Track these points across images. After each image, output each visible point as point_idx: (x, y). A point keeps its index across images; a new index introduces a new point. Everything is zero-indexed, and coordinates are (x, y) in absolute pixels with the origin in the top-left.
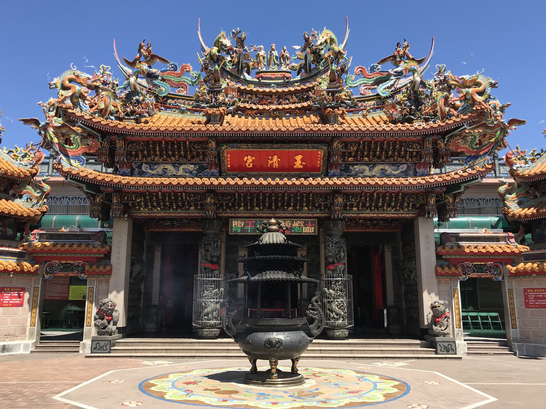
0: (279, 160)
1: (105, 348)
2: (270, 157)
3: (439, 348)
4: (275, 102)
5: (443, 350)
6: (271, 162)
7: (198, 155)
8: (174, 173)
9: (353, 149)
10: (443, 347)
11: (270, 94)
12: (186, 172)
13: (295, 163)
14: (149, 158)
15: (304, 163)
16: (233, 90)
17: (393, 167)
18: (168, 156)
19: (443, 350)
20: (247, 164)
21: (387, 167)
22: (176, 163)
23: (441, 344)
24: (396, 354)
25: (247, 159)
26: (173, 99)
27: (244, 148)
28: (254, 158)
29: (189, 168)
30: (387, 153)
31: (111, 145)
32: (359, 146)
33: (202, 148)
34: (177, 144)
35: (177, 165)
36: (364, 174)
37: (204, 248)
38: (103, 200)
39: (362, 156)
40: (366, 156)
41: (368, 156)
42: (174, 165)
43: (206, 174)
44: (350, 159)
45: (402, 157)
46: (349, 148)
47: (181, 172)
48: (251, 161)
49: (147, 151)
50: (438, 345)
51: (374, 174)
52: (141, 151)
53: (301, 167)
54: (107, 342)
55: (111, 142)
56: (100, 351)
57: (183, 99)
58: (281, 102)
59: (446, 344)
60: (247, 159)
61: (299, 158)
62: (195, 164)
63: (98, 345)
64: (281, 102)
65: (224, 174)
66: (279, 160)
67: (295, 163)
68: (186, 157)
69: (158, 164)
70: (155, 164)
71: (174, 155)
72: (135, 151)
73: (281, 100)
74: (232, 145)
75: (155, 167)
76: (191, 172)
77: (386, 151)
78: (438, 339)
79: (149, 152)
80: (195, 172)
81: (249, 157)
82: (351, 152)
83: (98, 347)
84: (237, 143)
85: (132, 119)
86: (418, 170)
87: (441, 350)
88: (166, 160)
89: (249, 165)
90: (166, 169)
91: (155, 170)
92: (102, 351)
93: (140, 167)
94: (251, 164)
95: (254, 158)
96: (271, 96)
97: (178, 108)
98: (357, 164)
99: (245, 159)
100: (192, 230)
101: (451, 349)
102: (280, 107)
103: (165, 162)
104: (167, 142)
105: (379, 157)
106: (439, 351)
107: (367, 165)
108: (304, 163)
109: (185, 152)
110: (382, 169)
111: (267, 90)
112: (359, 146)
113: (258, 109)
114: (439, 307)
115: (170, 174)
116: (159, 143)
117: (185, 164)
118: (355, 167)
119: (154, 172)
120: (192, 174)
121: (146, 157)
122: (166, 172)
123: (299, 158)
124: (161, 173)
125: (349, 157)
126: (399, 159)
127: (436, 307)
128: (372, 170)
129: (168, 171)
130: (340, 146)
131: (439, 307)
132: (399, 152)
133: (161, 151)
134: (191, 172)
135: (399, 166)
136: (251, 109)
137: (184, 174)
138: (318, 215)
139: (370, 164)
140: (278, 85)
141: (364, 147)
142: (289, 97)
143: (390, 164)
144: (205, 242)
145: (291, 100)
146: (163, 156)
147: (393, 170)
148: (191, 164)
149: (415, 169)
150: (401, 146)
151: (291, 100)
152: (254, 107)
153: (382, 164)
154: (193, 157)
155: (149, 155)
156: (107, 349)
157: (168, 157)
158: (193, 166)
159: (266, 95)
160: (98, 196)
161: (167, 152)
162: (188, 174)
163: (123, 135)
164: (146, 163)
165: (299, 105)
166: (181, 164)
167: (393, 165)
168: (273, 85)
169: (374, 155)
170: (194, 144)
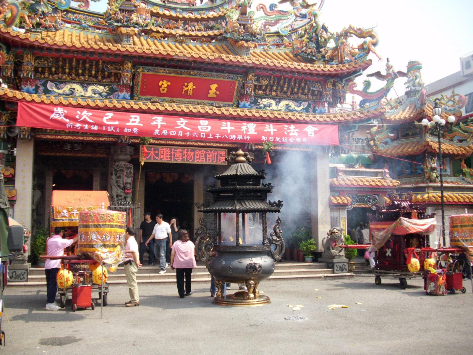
0: (194, 87)
1: (22, 277)
2: (186, 84)
3: (335, 268)
4: (181, 28)
5: (338, 269)
6: (186, 89)
7: (109, 75)
8: (83, 94)
9: (265, 82)
10: (339, 267)
11: (177, 19)
12: (95, 94)
13: (210, 91)
14: (56, 76)
15: (218, 93)
16: (147, 12)
17: (296, 103)
18: (78, 75)
19: (338, 269)
20: (161, 89)
21: (291, 103)
22: (84, 83)
23: (337, 264)
24: (301, 274)
25: (162, 84)
26: (73, 13)
27: (161, 72)
28: (169, 83)
29: (98, 89)
30: (293, 89)
31: (16, 58)
32: (270, 80)
33: (116, 69)
34: (89, 63)
35: (85, 85)
36: (271, 108)
37: (116, 175)
38: (9, 119)
39: (271, 91)
40: (274, 91)
41: (276, 91)
42: (82, 84)
43: (116, 97)
44: (260, 92)
45: (305, 95)
46: (261, 81)
47: (89, 93)
48: (166, 85)
49: (56, 69)
50: (335, 266)
51: (279, 108)
52: (48, 68)
53: (215, 96)
54: (24, 271)
55: (16, 56)
56: (17, 280)
57: (84, 15)
58: (186, 28)
59: (341, 265)
60: (162, 84)
61: (214, 87)
62: (105, 86)
63: (14, 274)
64: (186, 28)
65: (136, 98)
66: (194, 87)
67: (210, 91)
68: (96, 77)
69: (65, 82)
70: (61, 83)
71: (83, 74)
72: (42, 68)
73: (187, 26)
74: (149, 67)
75: (61, 85)
76: (100, 94)
77: (302, 88)
78: (335, 260)
79: (57, 69)
80: (105, 94)
81: (165, 82)
82: (262, 86)
83: (14, 276)
84: (152, 66)
85: (38, 32)
86: (317, 108)
87: (337, 270)
88: (75, 79)
89: (163, 90)
90: (74, 89)
91: (62, 88)
92: (19, 280)
93: (45, 85)
94: (166, 89)
95: (169, 83)
96: (177, 21)
97: (79, 23)
98: (265, 98)
99: (160, 84)
100: (86, 155)
101: (345, 268)
102: (187, 33)
103: (73, 81)
104: (78, 61)
105: (285, 93)
106: (335, 271)
107: (274, 98)
108: (218, 93)
109: (97, 71)
110: (287, 105)
111: (174, 14)
112: (270, 80)
113: (164, 33)
114: (337, 232)
115: (77, 95)
116: (69, 61)
117: (93, 84)
118: (263, 100)
119: (61, 91)
120: (102, 96)
121: (53, 75)
122: (73, 93)
123: (214, 87)
124: (68, 92)
125: (259, 90)
126: (303, 96)
127: (335, 233)
128: (278, 105)
129: (76, 91)
130: (254, 78)
131: (337, 232)
132: (303, 89)
133: (71, 69)
134: (100, 94)
135: (301, 103)
136: (158, 32)
137: (93, 95)
138: (229, 145)
139: (276, 99)
140: (184, 10)
141: (274, 82)
142: (196, 24)
143: (293, 100)
144: (117, 168)
145: (197, 27)
146: (71, 75)
147: (296, 106)
148: (101, 85)
149: (314, 107)
150: (306, 84)
151: (197, 27)
152: (161, 30)
153: (286, 99)
154: (103, 78)
155: (56, 73)
156: (24, 278)
157: (76, 75)
158: (102, 87)
159: (172, 20)
160: (4, 114)
161: (77, 70)
162: (97, 96)
163: (31, 47)
164: (52, 81)
165: (205, 33)
166: (90, 84)
167: (296, 101)
168: (178, 10)
169: (282, 90)
170: (107, 64)
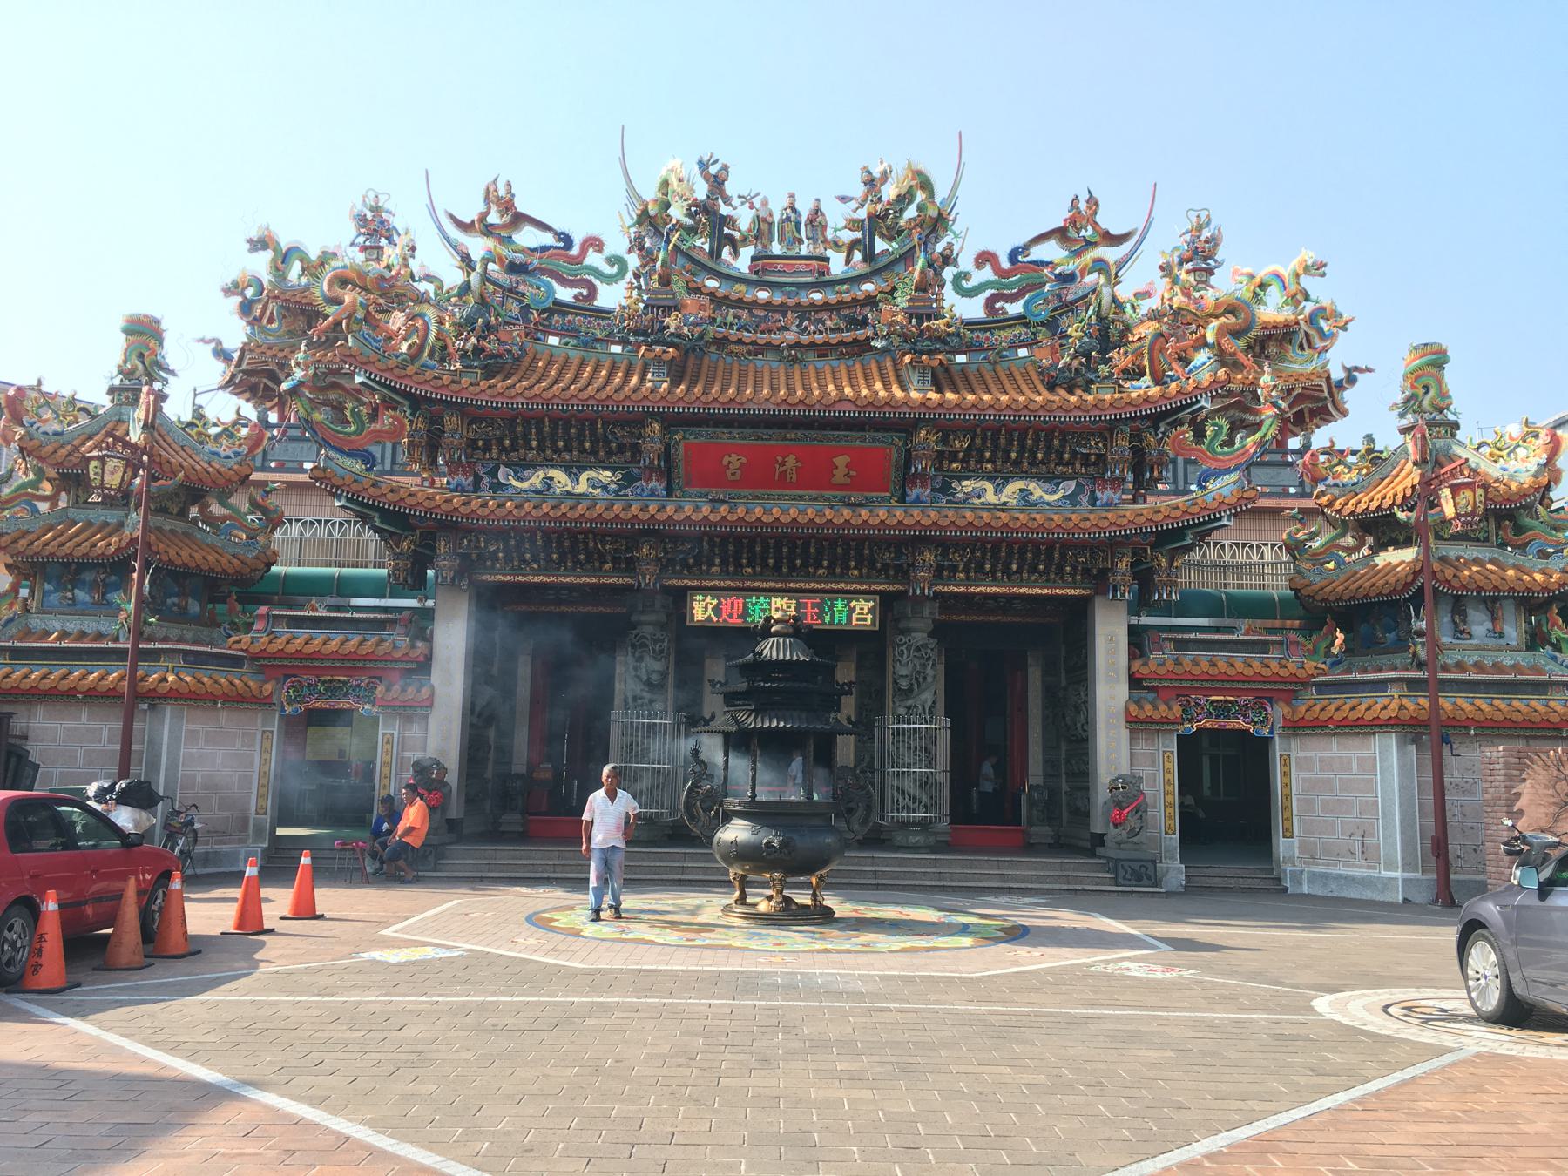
3: (1121, 873)
4: (794, 328)
7: (621, 449)
8: (569, 488)
9: (960, 444)
12: (594, 487)
15: (853, 473)
17: (1046, 486)
20: (728, 472)
21: (1032, 486)
23: (1126, 864)
27: (725, 436)
28: (744, 460)
30: (1033, 454)
31: (431, 424)
33: (632, 434)
35: (575, 470)
39: (981, 460)
42: (567, 470)
45: (1067, 464)
48: (737, 465)
51: (1004, 499)
59: (1136, 866)
61: (841, 461)
62: (613, 470)
65: (678, 493)
68: (594, 452)
70: (526, 467)
71: (568, 449)
76: (605, 488)
86: (1098, 494)
90: (551, 479)
93: (493, 473)
96: (785, 315)
98: (968, 478)
99: (725, 462)
107: (990, 479)
108: (853, 473)
109: (594, 442)
112: (973, 439)
118: (965, 483)
119: (525, 485)
122: (550, 487)
123: (841, 461)
132: (1060, 454)
133: (541, 441)
134: (605, 488)
136: (740, 342)
141: (984, 440)
145: (829, 324)
148: (606, 469)
149: (1093, 492)
150: (1064, 441)
151: (829, 324)
154: (610, 453)
155: (514, 448)
158: (609, 474)
161: (554, 442)
164: (507, 466)
166: (583, 469)
167: (1047, 480)
